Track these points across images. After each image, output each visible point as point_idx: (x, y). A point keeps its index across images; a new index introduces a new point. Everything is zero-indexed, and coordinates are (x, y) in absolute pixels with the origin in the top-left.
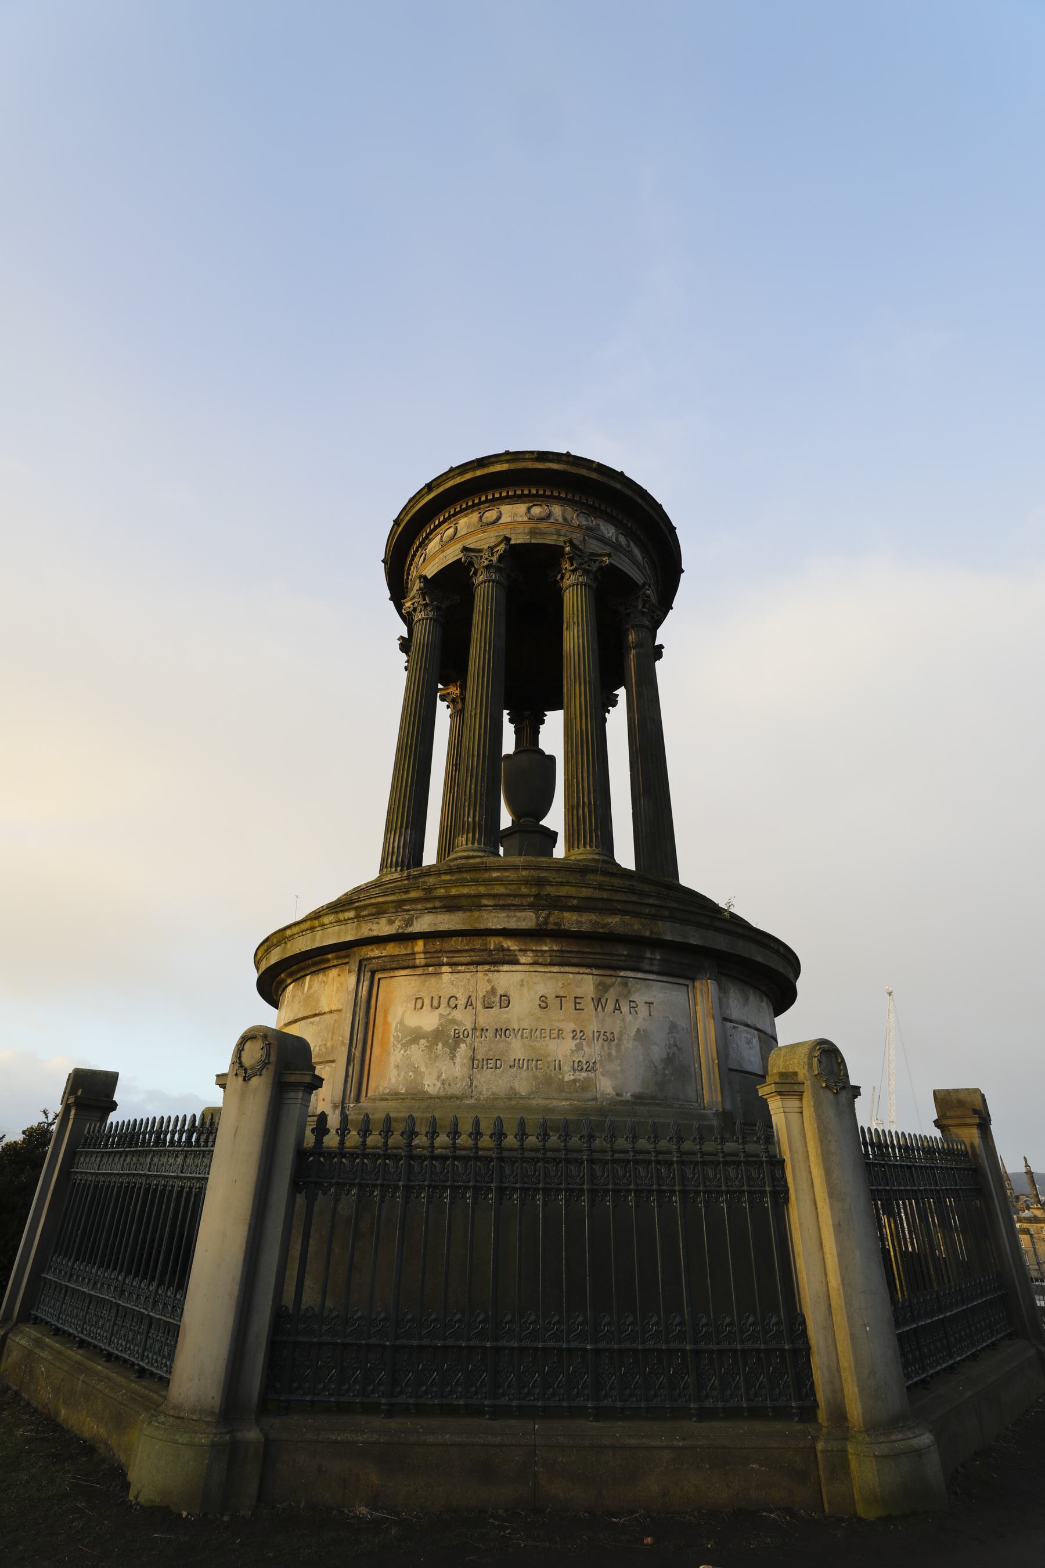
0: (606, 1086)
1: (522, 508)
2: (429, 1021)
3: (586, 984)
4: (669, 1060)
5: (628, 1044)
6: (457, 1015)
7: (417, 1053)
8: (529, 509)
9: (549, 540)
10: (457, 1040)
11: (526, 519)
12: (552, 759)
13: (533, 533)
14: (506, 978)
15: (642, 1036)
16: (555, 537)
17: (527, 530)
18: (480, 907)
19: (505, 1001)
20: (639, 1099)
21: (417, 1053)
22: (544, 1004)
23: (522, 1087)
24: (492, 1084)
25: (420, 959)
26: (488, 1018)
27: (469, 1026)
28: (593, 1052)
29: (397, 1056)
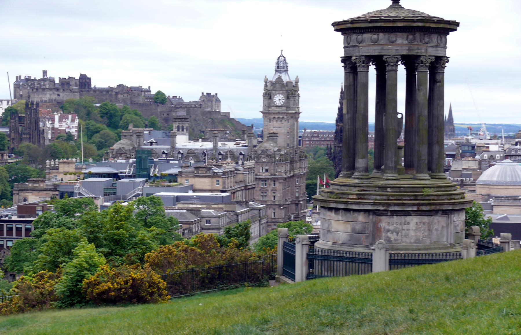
1: (405, 35)
3: (426, 219)
5: (433, 231)
6: (398, 226)
7: (389, 234)
8: (408, 36)
9: (414, 53)
11: (407, 42)
12: (402, 114)
13: (409, 50)
14: (408, 219)
15: (437, 230)
16: (416, 51)
17: (407, 48)
18: (405, 205)
19: (409, 223)
22: (417, 223)
25: (389, 214)
26: (405, 227)
27: (400, 228)
29: (383, 234)
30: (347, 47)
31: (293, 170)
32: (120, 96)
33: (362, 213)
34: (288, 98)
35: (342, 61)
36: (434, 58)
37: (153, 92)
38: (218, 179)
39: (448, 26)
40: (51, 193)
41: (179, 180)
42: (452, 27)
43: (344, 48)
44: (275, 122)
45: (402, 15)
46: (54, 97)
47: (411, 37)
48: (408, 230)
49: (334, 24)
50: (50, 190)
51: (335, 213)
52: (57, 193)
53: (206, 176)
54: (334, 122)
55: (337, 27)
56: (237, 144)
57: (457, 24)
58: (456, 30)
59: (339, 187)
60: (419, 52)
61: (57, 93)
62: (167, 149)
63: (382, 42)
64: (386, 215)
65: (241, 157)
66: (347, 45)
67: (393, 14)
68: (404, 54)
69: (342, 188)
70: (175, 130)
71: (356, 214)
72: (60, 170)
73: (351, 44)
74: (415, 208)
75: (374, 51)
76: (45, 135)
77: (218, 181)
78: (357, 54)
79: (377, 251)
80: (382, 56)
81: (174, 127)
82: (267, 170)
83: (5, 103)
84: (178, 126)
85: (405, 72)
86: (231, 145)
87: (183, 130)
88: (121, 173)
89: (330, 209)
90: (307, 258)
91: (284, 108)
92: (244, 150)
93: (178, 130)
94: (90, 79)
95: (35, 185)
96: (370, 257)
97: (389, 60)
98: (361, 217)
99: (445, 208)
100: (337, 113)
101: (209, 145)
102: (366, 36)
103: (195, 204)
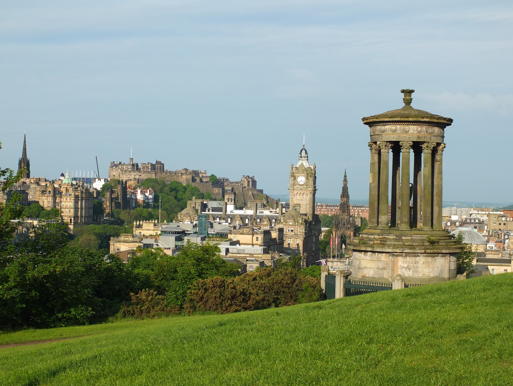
0: (432, 275)
1: (415, 127)
2: (406, 265)
3: (430, 259)
4: (441, 270)
10: (410, 269)
13: (418, 137)
14: (418, 259)
15: (438, 267)
20: (436, 276)
21: (404, 270)
22: (424, 263)
23: (420, 275)
24: (416, 275)
28: (430, 270)
29: (400, 270)
30: (373, 135)
31: (311, 231)
32: (184, 177)
33: (384, 254)
34: (307, 179)
35: (369, 146)
36: (435, 144)
37: (209, 174)
38: (257, 236)
39: (446, 122)
40: (137, 244)
41: (229, 236)
42: (449, 123)
43: (371, 136)
44: (298, 196)
45: (413, 113)
46: (137, 177)
47: (419, 129)
48: (417, 267)
49: (363, 119)
50: (136, 242)
51: (364, 254)
52: (141, 244)
53: (249, 234)
54: (339, 198)
55: (365, 121)
56: (271, 212)
57: (451, 121)
58: (451, 125)
59: (367, 236)
60: (425, 140)
61: (139, 174)
62: (220, 215)
63: (398, 132)
64: (402, 256)
65: (274, 221)
66: (373, 134)
67: (407, 112)
68: (415, 140)
69: (370, 236)
70: (226, 201)
71: (380, 255)
72: (144, 228)
73: (376, 133)
74: (423, 251)
75: (394, 138)
76: (131, 204)
77: (257, 238)
78: (381, 140)
79: (396, 281)
80: (399, 142)
81: (225, 199)
82: (292, 231)
83: (103, 180)
84: (228, 199)
85: (413, 154)
86: (266, 212)
87: (231, 201)
88: (187, 231)
89: (360, 251)
90: (344, 287)
91: (305, 186)
92: (275, 216)
93: (228, 201)
94: (163, 164)
95: (126, 239)
96: (390, 286)
97: (404, 145)
98: (383, 257)
99: (444, 251)
100: (342, 190)
101: (250, 212)
102: (388, 127)
103: (241, 254)
